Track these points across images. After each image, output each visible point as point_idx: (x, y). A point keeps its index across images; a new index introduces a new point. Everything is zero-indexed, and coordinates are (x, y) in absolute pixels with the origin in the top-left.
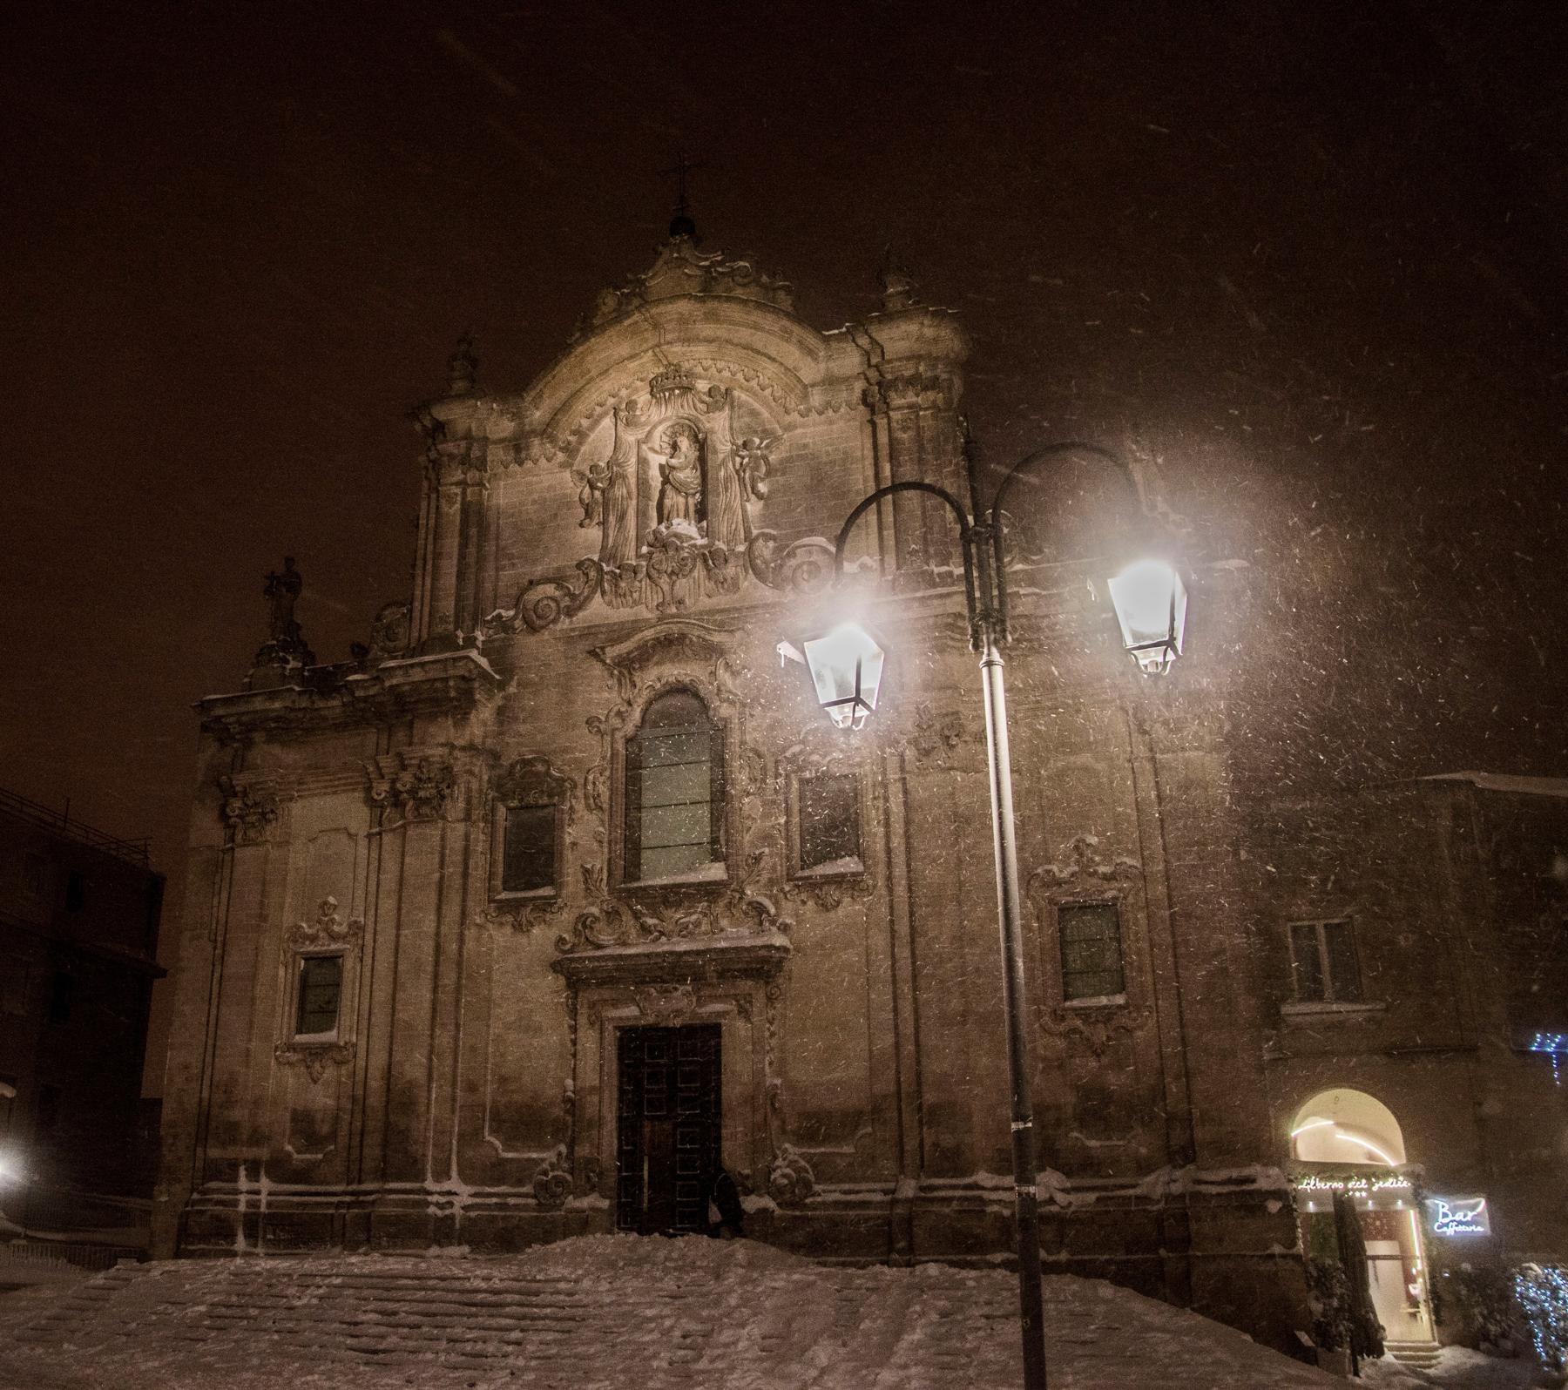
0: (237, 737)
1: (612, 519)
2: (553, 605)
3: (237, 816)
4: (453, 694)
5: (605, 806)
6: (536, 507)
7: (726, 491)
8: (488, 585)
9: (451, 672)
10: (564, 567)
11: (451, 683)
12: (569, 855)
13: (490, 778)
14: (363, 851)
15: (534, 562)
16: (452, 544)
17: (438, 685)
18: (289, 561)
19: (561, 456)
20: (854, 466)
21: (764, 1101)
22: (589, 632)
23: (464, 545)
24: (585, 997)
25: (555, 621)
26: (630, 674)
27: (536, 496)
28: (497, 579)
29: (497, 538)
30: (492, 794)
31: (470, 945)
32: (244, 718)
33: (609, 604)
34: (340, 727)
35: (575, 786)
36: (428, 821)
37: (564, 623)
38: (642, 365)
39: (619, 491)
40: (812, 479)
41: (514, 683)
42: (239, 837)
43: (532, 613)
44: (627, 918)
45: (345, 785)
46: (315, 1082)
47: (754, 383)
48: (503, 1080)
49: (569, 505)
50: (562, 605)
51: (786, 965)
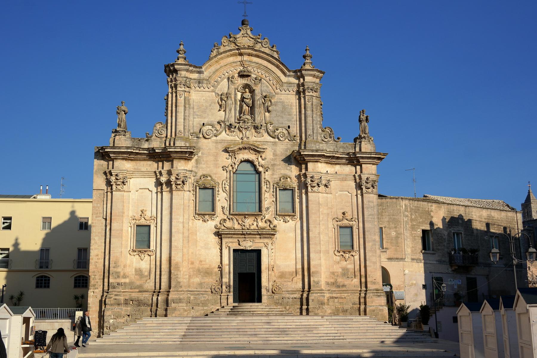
2: (212, 132)
5: (228, 191)
6: (205, 101)
7: (260, 108)
10: (213, 121)
14: (154, 195)
15: (205, 118)
16: (181, 109)
19: (212, 88)
20: (294, 107)
21: (271, 268)
22: (222, 141)
23: (185, 110)
25: (212, 137)
26: (235, 155)
27: (204, 98)
28: (193, 122)
29: (193, 108)
30: (195, 184)
31: (190, 224)
36: (180, 191)
37: (214, 138)
38: (237, 65)
39: (229, 102)
40: (283, 109)
41: (200, 153)
44: (235, 221)
45: (147, 176)
48: (201, 261)
50: (214, 133)
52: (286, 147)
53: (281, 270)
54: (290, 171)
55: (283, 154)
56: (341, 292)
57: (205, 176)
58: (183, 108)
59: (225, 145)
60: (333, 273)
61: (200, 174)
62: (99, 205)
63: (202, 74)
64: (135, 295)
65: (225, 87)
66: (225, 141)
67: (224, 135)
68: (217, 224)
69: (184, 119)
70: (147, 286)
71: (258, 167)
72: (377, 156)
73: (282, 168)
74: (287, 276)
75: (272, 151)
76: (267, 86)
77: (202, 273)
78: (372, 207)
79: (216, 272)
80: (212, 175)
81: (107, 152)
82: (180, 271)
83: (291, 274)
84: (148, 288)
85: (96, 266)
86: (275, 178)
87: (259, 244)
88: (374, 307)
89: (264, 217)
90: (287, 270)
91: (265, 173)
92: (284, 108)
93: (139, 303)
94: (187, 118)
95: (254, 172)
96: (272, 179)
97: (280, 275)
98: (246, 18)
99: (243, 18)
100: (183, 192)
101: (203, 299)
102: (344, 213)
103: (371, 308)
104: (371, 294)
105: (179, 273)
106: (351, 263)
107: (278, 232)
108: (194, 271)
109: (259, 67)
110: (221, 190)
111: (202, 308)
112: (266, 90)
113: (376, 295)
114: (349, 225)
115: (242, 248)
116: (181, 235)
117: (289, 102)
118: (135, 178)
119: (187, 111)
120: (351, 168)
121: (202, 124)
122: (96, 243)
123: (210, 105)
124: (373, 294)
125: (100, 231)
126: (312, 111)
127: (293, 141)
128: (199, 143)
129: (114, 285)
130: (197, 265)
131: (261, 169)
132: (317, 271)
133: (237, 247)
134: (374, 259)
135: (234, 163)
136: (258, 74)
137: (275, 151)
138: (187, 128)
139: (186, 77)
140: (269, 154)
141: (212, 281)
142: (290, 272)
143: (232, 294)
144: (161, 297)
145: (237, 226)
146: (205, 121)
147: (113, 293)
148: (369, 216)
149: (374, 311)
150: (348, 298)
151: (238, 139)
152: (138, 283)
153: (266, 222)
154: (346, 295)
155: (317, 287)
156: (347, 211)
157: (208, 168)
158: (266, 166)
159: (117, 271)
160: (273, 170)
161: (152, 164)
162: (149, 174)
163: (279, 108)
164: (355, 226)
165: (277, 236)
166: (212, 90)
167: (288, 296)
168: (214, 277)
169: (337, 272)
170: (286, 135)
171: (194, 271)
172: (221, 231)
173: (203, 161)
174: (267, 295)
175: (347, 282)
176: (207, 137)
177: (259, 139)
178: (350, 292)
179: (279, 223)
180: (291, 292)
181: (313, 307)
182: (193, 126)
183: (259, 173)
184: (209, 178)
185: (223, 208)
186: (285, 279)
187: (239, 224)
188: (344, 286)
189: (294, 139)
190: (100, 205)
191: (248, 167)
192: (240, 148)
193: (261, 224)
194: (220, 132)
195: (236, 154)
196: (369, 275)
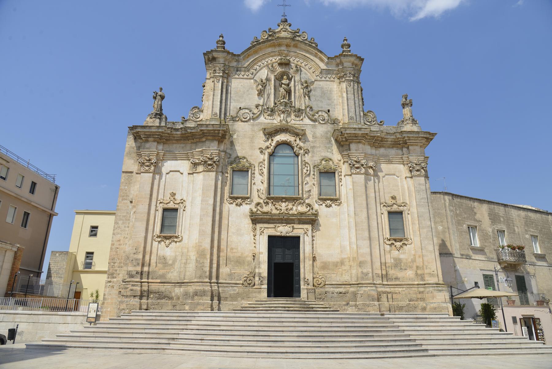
0: (143, 139)
1: (266, 96)
2: (248, 115)
3: (142, 163)
4: (220, 135)
6: (242, 87)
8: (228, 107)
9: (221, 128)
11: (220, 132)
13: (228, 161)
15: (242, 102)
17: (217, 132)
18: (161, 89)
19: (250, 75)
24: (259, 226)
29: (231, 94)
32: (147, 133)
33: (265, 118)
34: (178, 141)
35: (255, 167)
41: (236, 135)
43: (241, 116)
46: (167, 247)
47: (307, 67)
48: (232, 249)
51: (317, 222)
52: (326, 130)
54: (331, 153)
55: (323, 136)
56: (395, 286)
58: (220, 91)
59: (263, 127)
62: (126, 187)
63: (240, 63)
65: (263, 74)
66: (262, 124)
68: (252, 208)
69: (221, 102)
70: (171, 276)
72: (425, 136)
73: (322, 150)
74: (330, 267)
75: (311, 133)
76: (306, 74)
77: (233, 262)
78: (423, 190)
80: (247, 157)
81: (137, 133)
82: (207, 259)
83: (336, 265)
84: (172, 278)
85: (117, 252)
86: (315, 161)
87: (297, 230)
88: (436, 304)
89: (303, 201)
90: (330, 260)
91: (304, 155)
93: (161, 296)
94: (224, 101)
95: (293, 155)
96: (311, 161)
97: (322, 266)
100: (214, 173)
103: (432, 305)
104: (431, 289)
105: (205, 261)
106: (403, 253)
107: (320, 217)
108: (224, 260)
109: (297, 56)
110: (257, 172)
111: (231, 303)
112: (305, 77)
113: (437, 290)
114: (399, 210)
115: (278, 234)
117: (328, 87)
118: (165, 160)
120: (396, 151)
121: (239, 108)
122: (119, 227)
123: (248, 90)
124: (433, 288)
125: (125, 214)
127: (333, 124)
128: (235, 125)
129: (133, 273)
132: (365, 261)
133: (273, 233)
135: (271, 145)
136: (296, 63)
137: (314, 133)
139: (223, 63)
141: (244, 271)
142: (334, 262)
143: (266, 286)
144: (183, 289)
145: (275, 212)
147: (130, 283)
148: (421, 199)
149: (435, 308)
150: (404, 293)
151: (275, 122)
152: (161, 272)
154: (400, 289)
155: (367, 279)
157: (244, 150)
158: (305, 148)
159: (138, 258)
161: (185, 146)
162: (180, 156)
164: (406, 212)
166: (250, 77)
167: (332, 289)
168: (246, 267)
169: (389, 263)
171: (224, 260)
172: (255, 216)
173: (239, 143)
174: (307, 289)
175: (400, 274)
176: (243, 120)
177: (298, 122)
178: (405, 286)
180: (335, 286)
181: (362, 304)
182: (230, 110)
184: (245, 160)
185: (258, 191)
186: (328, 271)
187: (276, 209)
188: (397, 279)
189: (334, 121)
190: (128, 187)
192: (277, 130)
193: (302, 209)
194: (257, 115)
195: (273, 136)
196: (427, 266)
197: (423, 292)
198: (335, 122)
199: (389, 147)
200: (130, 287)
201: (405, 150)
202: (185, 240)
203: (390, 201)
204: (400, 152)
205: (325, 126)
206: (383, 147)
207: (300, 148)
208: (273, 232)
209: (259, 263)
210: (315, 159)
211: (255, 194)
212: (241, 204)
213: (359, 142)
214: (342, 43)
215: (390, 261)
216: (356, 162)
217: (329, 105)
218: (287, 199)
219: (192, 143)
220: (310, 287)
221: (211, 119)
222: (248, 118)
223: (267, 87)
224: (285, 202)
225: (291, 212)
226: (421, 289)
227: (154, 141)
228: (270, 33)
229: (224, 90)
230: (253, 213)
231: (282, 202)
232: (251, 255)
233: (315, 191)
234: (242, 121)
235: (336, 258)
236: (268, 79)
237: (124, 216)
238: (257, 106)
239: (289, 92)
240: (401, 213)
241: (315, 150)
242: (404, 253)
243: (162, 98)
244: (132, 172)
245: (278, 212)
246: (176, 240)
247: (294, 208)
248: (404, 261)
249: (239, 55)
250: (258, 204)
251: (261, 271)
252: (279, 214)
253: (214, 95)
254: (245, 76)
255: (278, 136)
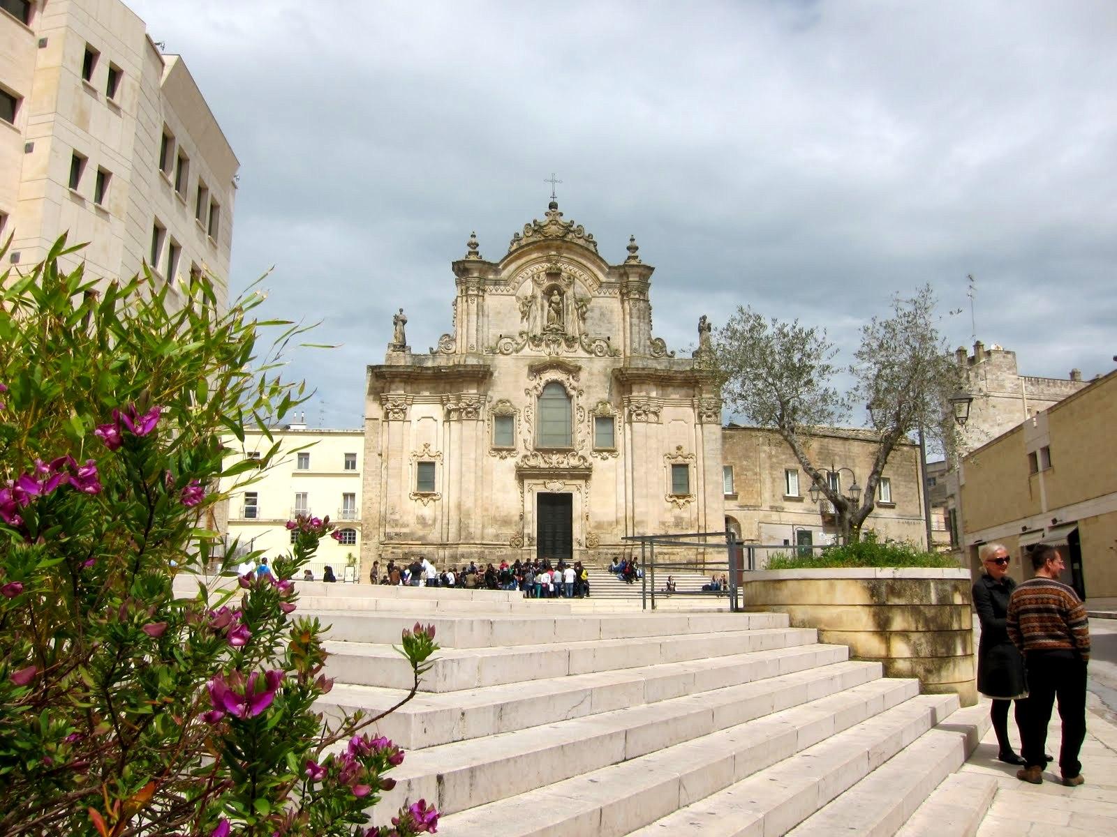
1: (531, 319)
8: (485, 334)
12: (519, 436)
15: (502, 329)
18: (401, 310)
19: (512, 291)
22: (525, 357)
24: (526, 482)
25: (512, 352)
29: (488, 316)
31: (485, 462)
37: (514, 354)
42: (391, 415)
44: (540, 457)
48: (498, 508)
49: (515, 309)
53: (598, 520)
57: (501, 401)
58: (476, 316)
59: (528, 362)
60: (663, 523)
61: (495, 399)
64: (415, 549)
67: (529, 351)
69: (477, 330)
71: (569, 389)
76: (581, 287)
79: (516, 522)
80: (511, 399)
83: (610, 524)
92: (602, 314)
94: (480, 329)
98: (556, 200)
99: (552, 200)
101: (499, 554)
102: (679, 448)
105: (470, 521)
110: (522, 419)
115: (548, 491)
116: (473, 475)
119: (480, 321)
126: (639, 318)
130: (492, 512)
131: (573, 393)
134: (715, 506)
138: (480, 341)
140: (583, 375)
141: (510, 532)
143: (536, 548)
145: (543, 465)
146: (504, 332)
151: (544, 355)
152: (421, 533)
153: (579, 460)
156: (681, 444)
158: (580, 388)
160: (589, 393)
163: (596, 314)
165: (594, 476)
167: (606, 550)
168: (514, 527)
170: (606, 349)
176: (505, 352)
179: (597, 463)
183: (570, 398)
184: (508, 404)
185: (525, 441)
187: (545, 462)
191: (553, 391)
193: (574, 462)
197: (703, 554)
198: (614, 354)
199: (679, 386)
200: (390, 550)
201: (697, 389)
202: (445, 499)
203: (674, 452)
204: (691, 392)
205: (603, 359)
206: (672, 386)
207: (574, 388)
208: (542, 490)
209: (529, 523)
210: (590, 401)
211: (520, 445)
212: (506, 457)
213: (643, 383)
214: (629, 243)
215: (670, 519)
216: (637, 407)
217: (609, 330)
218: (560, 451)
219: (445, 383)
220: (583, 548)
221: (469, 354)
222: (511, 350)
223: (534, 307)
224: (556, 454)
225: (562, 466)
226: (701, 550)
227: (401, 382)
228: (536, 228)
229: (480, 313)
230: (520, 467)
231: (553, 454)
232: (518, 514)
233: (589, 443)
234: (504, 354)
235: (612, 518)
236: (534, 297)
237: (373, 472)
238: (521, 334)
239: (559, 312)
240: (686, 466)
241: (591, 390)
242: (685, 511)
243: (404, 322)
244: (377, 419)
245: (547, 466)
246: (434, 498)
247: (566, 462)
248: (686, 520)
249: (497, 265)
250: (525, 457)
251: (530, 531)
252: (550, 468)
253: (468, 321)
254: (505, 292)
255: (548, 374)
